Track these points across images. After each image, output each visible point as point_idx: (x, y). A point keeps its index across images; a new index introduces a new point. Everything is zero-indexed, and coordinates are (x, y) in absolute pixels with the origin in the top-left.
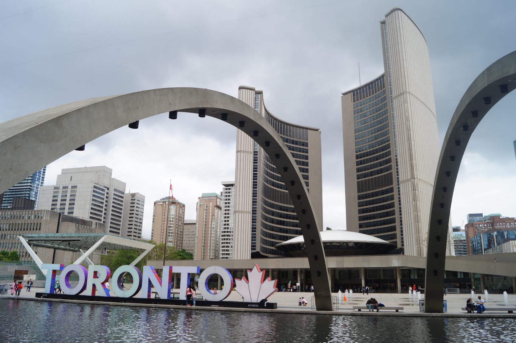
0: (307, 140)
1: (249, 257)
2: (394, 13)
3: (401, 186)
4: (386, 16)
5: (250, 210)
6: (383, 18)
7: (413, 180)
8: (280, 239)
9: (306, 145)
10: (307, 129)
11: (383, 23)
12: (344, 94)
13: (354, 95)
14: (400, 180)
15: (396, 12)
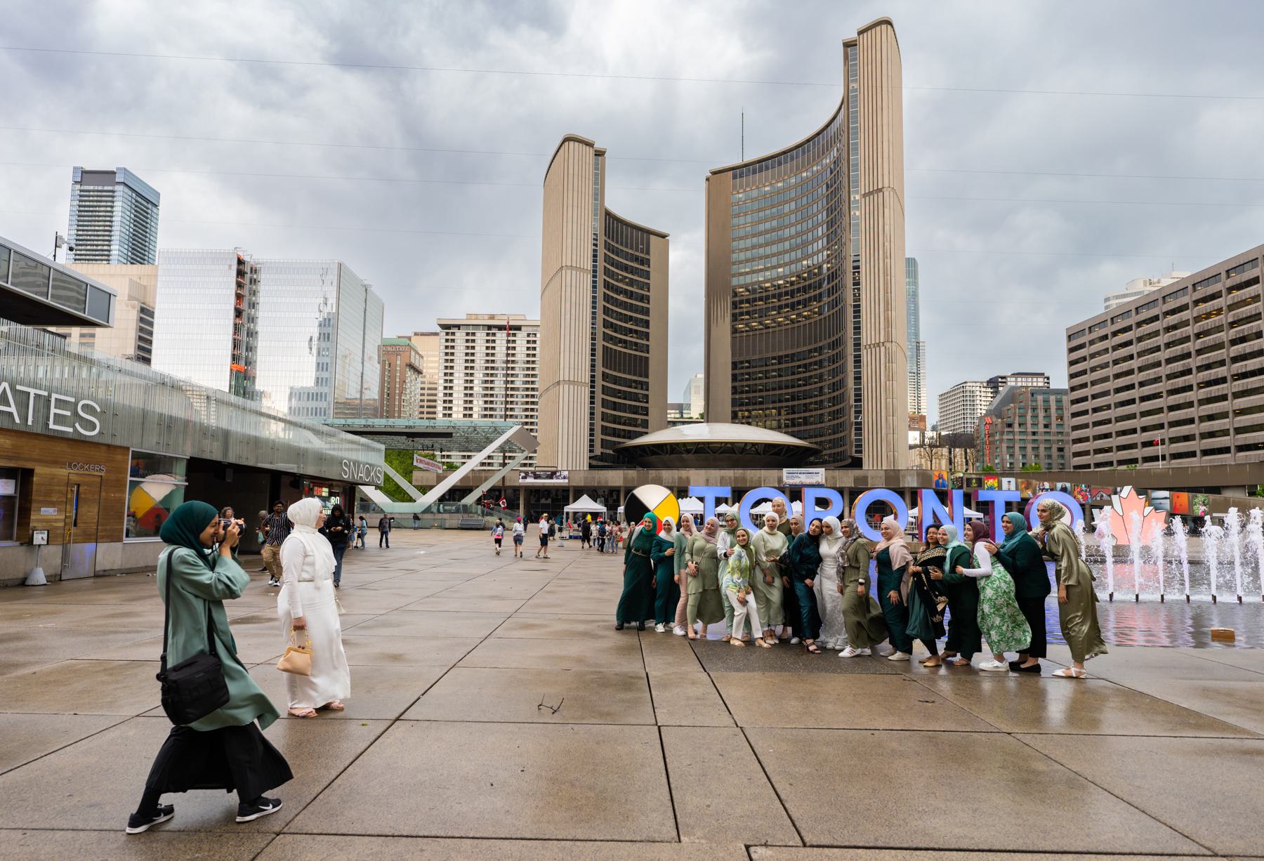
0: (648, 253)
1: (586, 468)
2: (878, 28)
3: (864, 352)
4: (860, 33)
5: (588, 380)
6: (853, 35)
7: (888, 345)
8: (624, 437)
9: (646, 262)
10: (649, 232)
11: (849, 45)
12: (714, 173)
13: (735, 177)
14: (863, 342)
15: (884, 27)
